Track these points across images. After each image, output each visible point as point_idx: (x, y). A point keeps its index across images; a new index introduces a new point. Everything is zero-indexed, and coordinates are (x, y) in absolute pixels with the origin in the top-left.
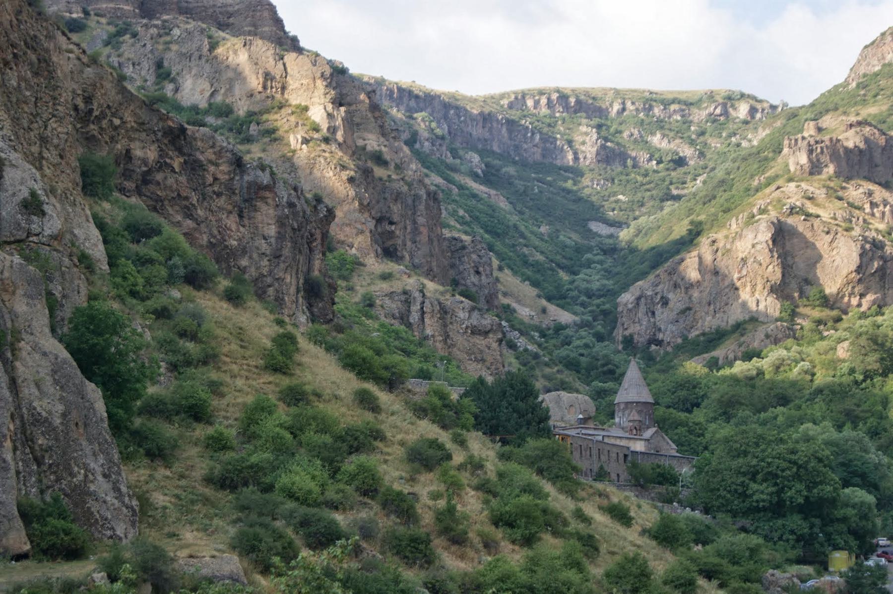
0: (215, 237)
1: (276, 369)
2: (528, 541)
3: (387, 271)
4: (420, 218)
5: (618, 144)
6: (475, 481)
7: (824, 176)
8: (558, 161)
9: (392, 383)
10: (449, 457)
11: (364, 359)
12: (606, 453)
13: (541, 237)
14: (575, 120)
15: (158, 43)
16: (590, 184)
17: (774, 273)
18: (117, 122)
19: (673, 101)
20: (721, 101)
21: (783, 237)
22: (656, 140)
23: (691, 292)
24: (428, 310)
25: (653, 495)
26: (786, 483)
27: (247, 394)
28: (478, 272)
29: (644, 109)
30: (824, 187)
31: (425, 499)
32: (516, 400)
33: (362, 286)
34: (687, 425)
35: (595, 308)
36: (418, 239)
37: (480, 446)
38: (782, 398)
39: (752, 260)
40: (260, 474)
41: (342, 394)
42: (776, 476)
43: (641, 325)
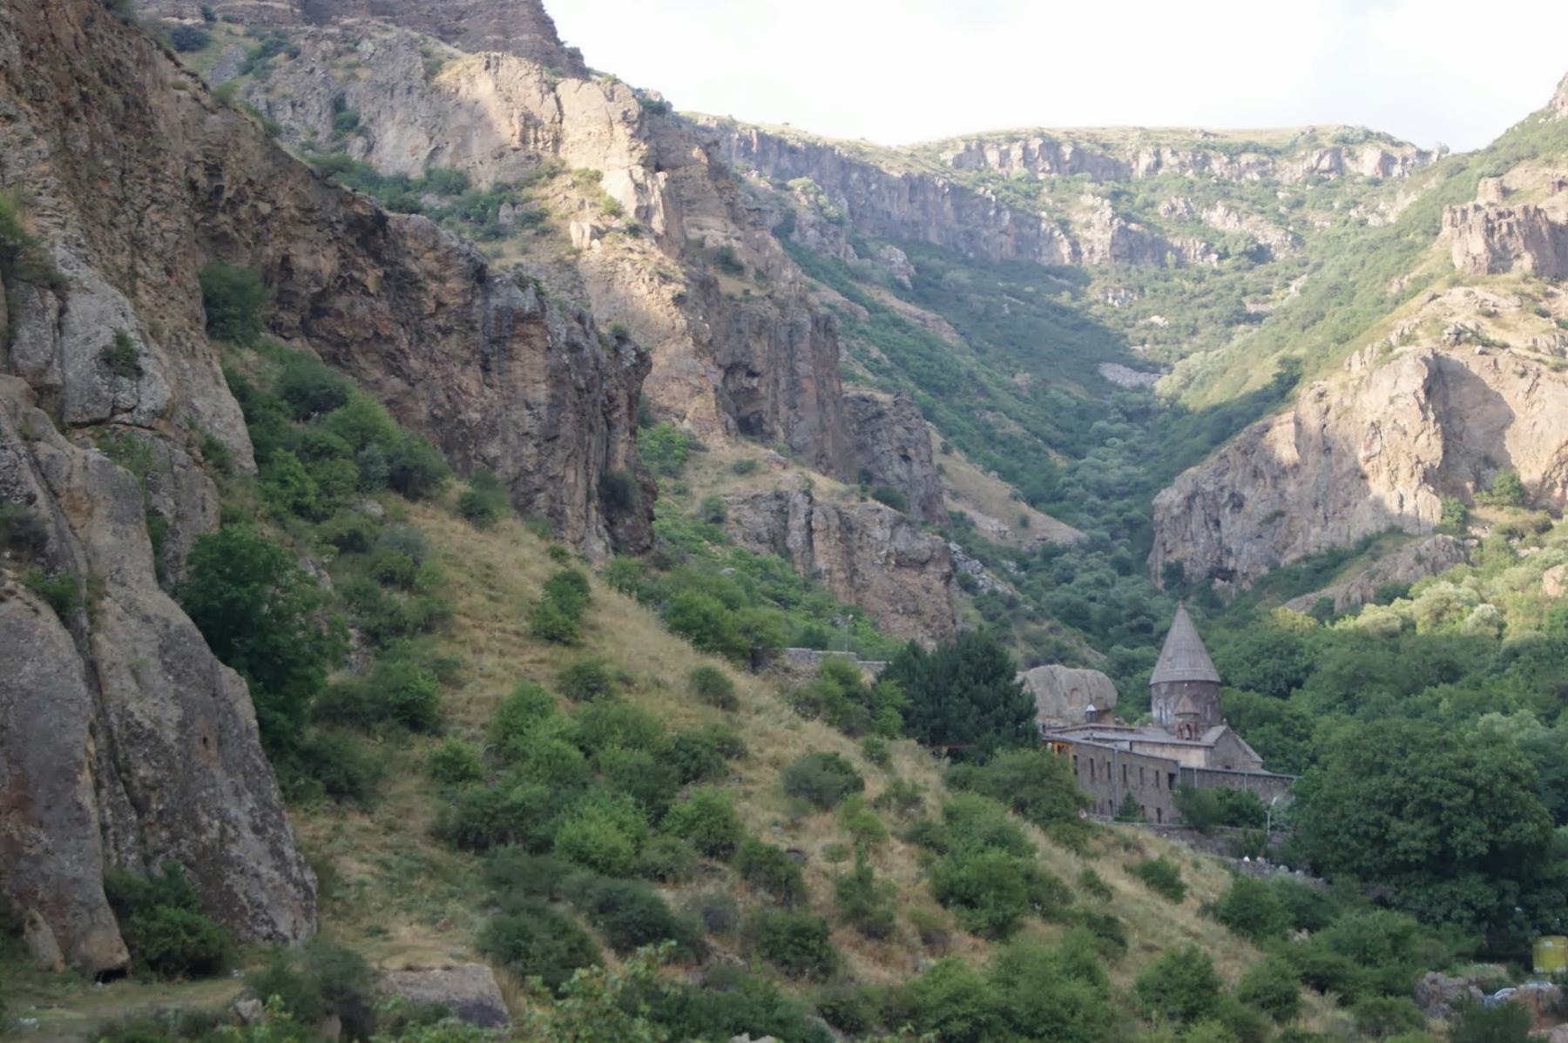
0: (441, 406)
1: (553, 637)
2: (1001, 930)
3: (746, 458)
4: (801, 364)
5: (1149, 225)
6: (906, 827)
7: (1514, 274)
9: (755, 658)
10: (858, 785)
11: (706, 617)
14: (1072, 185)
15: (335, 66)
16: (1101, 297)
17: (1431, 449)
18: (265, 208)
19: (1246, 148)
20: (1329, 145)
21: (1445, 385)
22: (1217, 217)
23: (1282, 484)
25: (1220, 844)
26: (1455, 818)
27: (503, 681)
28: (906, 458)
29: (1195, 162)
30: (1515, 293)
31: (817, 860)
32: (977, 682)
33: (702, 486)
34: (1280, 720)
35: (1112, 516)
36: (799, 401)
37: (915, 766)
38: (1447, 669)
39: (1390, 425)
40: (528, 821)
41: (669, 677)
42: (1438, 807)
43: (1196, 544)
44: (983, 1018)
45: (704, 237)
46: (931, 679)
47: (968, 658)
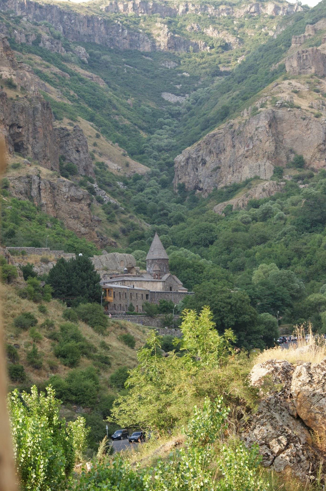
2: (73, 364)
3: (17, 163)
4: (37, 122)
5: (183, 35)
6: (49, 333)
8: (141, 49)
10: (36, 322)
12: (135, 295)
13: (127, 107)
14: (153, 19)
21: (276, 122)
22: (210, 31)
24: (43, 188)
25: (158, 320)
26: (225, 314)
28: (78, 151)
29: (201, 9)
30: (307, 83)
31: (23, 347)
35: (161, 161)
36: (37, 136)
37: (56, 310)
38: (263, 238)
42: (220, 311)
44: (63, 391)
45: (2, 75)
46: (67, 271)
47: (79, 264)
